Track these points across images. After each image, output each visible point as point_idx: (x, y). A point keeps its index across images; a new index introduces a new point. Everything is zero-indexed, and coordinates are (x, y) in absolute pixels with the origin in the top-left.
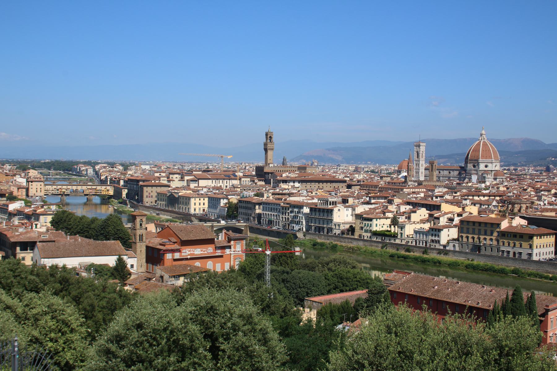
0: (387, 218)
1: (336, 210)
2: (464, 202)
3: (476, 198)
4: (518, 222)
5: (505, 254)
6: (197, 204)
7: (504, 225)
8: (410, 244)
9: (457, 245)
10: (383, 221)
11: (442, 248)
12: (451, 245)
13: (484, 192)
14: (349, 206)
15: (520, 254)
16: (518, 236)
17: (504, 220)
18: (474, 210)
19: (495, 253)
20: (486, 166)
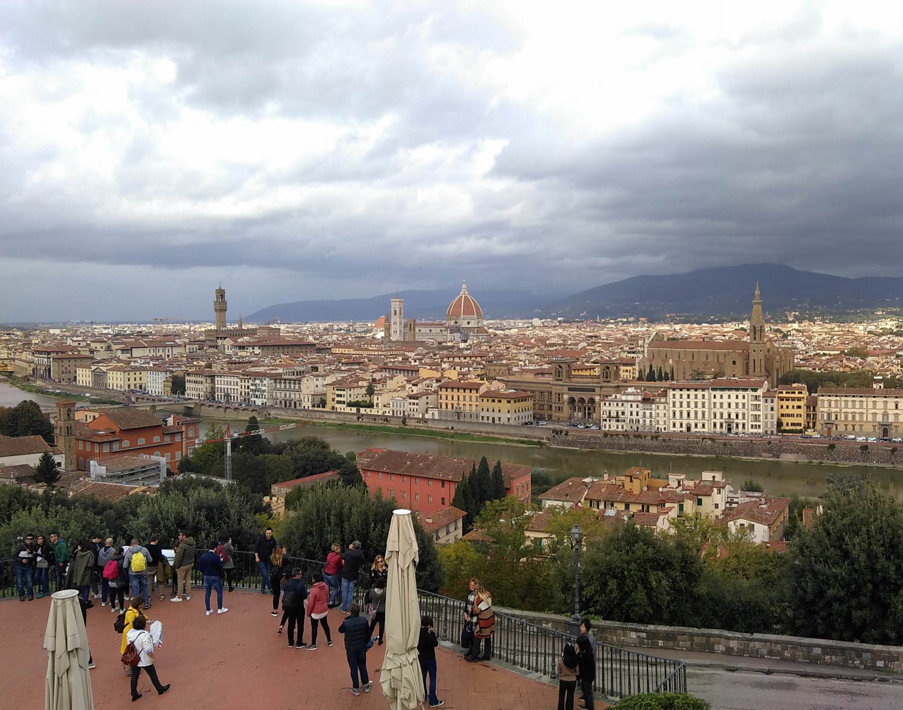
0: (361, 387)
1: (304, 380)
2: (444, 366)
3: (457, 360)
4: (496, 386)
5: (485, 419)
6: (132, 379)
7: (483, 390)
8: (387, 414)
9: (436, 413)
10: (357, 391)
11: (421, 416)
12: (430, 412)
13: (466, 352)
14: (319, 376)
15: (500, 419)
16: (496, 400)
17: (482, 384)
18: (453, 375)
19: (474, 420)
20: (469, 323)
